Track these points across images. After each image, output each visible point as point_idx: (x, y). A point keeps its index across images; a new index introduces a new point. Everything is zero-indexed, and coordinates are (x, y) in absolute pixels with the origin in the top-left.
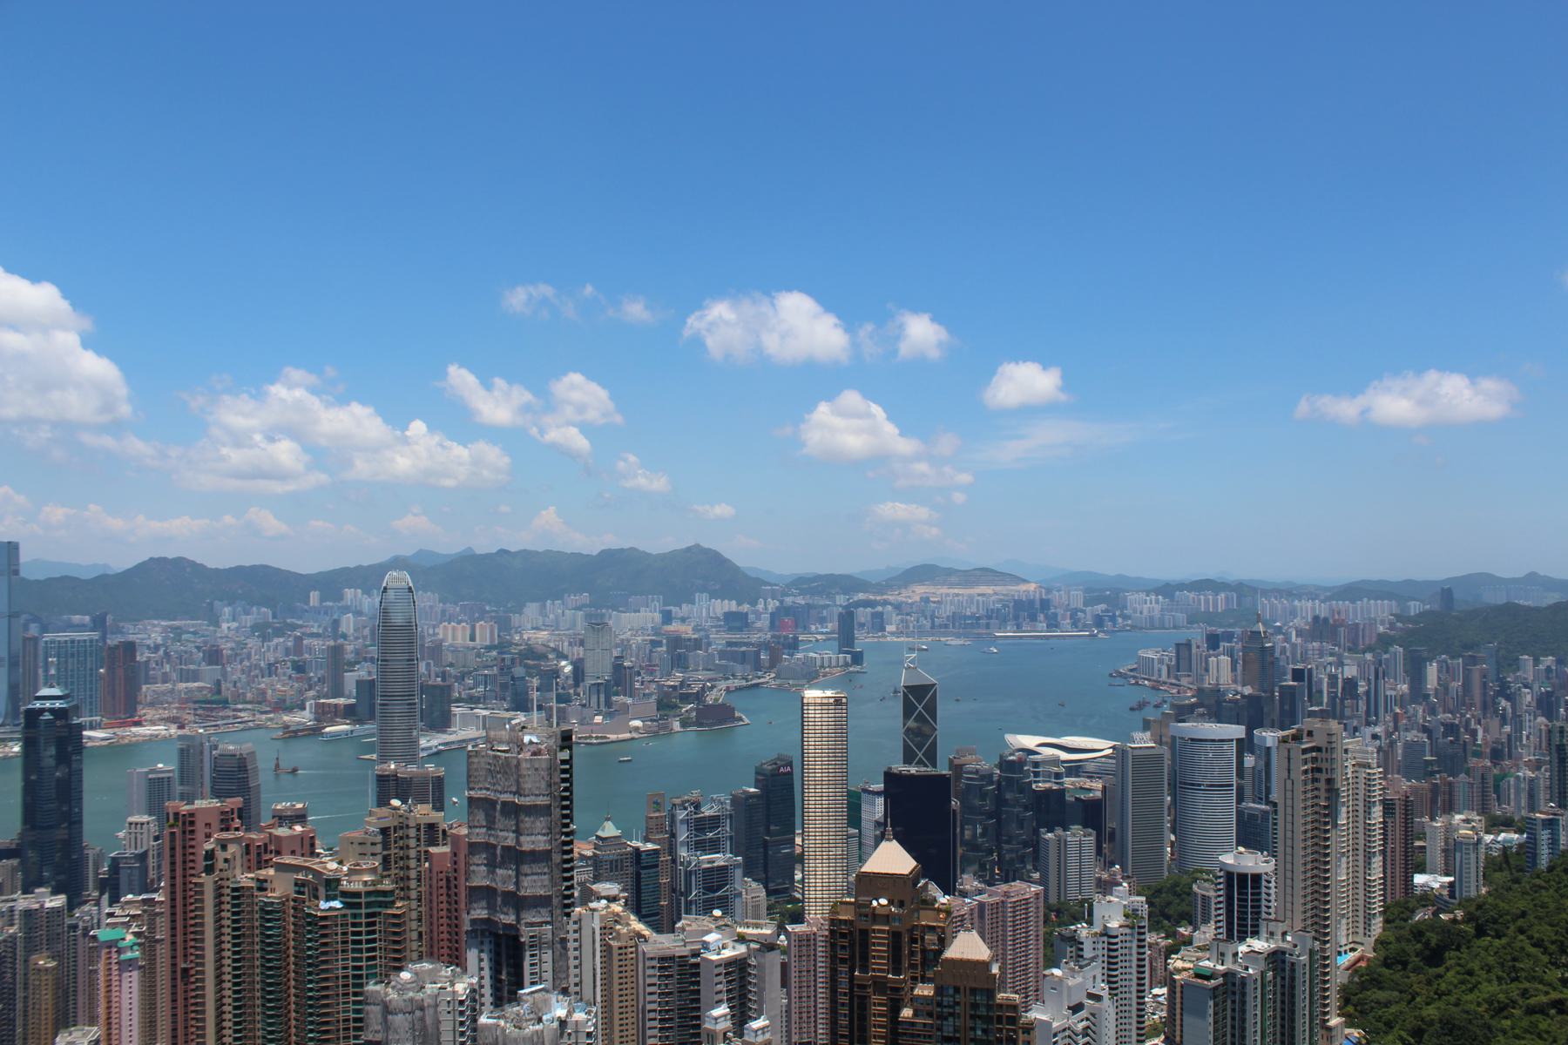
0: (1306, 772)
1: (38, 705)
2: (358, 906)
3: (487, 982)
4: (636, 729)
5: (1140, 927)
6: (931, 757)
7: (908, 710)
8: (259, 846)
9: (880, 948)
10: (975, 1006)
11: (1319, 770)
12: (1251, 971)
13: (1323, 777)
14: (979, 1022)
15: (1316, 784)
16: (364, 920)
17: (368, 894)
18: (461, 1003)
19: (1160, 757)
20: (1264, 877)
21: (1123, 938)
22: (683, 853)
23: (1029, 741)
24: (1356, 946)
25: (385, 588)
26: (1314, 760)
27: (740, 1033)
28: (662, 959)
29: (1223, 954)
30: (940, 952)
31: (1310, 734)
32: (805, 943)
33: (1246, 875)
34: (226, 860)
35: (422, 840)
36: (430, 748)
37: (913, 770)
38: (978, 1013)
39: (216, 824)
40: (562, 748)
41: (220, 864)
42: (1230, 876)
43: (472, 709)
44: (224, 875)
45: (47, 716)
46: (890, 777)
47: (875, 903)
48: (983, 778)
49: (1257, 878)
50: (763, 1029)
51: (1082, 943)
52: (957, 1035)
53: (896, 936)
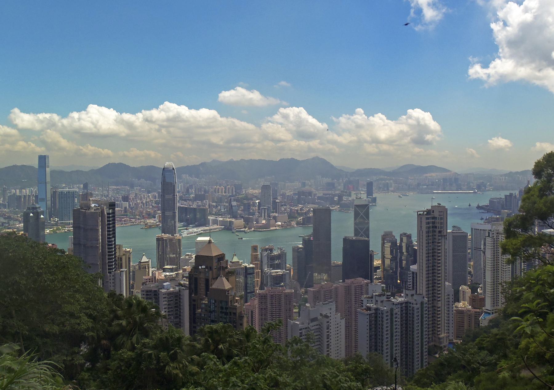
0: (429, 228)
4: (279, 226)
5: (387, 295)
9: (202, 285)
10: (222, 308)
11: (436, 227)
13: (437, 230)
14: (223, 314)
15: (435, 234)
26: (434, 223)
28: (147, 291)
29: (377, 301)
32: (263, 297)
36: (198, 232)
38: (223, 311)
43: (216, 218)
47: (200, 267)
51: (363, 301)
52: (216, 319)
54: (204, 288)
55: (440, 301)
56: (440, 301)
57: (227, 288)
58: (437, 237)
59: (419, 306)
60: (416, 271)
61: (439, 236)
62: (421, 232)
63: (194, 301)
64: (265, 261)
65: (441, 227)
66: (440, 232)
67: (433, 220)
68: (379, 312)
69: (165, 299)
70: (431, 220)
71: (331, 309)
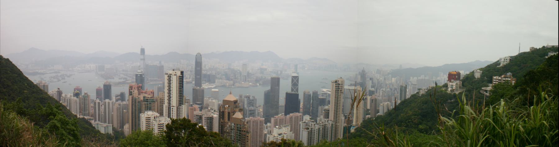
1: (137, 73)
2: (148, 101)
6: (297, 90)
7: (293, 81)
11: (339, 89)
12: (316, 128)
13: (340, 90)
26: (338, 86)
29: (312, 125)
41: (133, 94)
45: (139, 75)
46: (287, 94)
55: (339, 123)
56: (339, 123)
59: (331, 125)
61: (340, 93)
65: (342, 89)
66: (341, 91)
68: (313, 130)
70: (337, 85)
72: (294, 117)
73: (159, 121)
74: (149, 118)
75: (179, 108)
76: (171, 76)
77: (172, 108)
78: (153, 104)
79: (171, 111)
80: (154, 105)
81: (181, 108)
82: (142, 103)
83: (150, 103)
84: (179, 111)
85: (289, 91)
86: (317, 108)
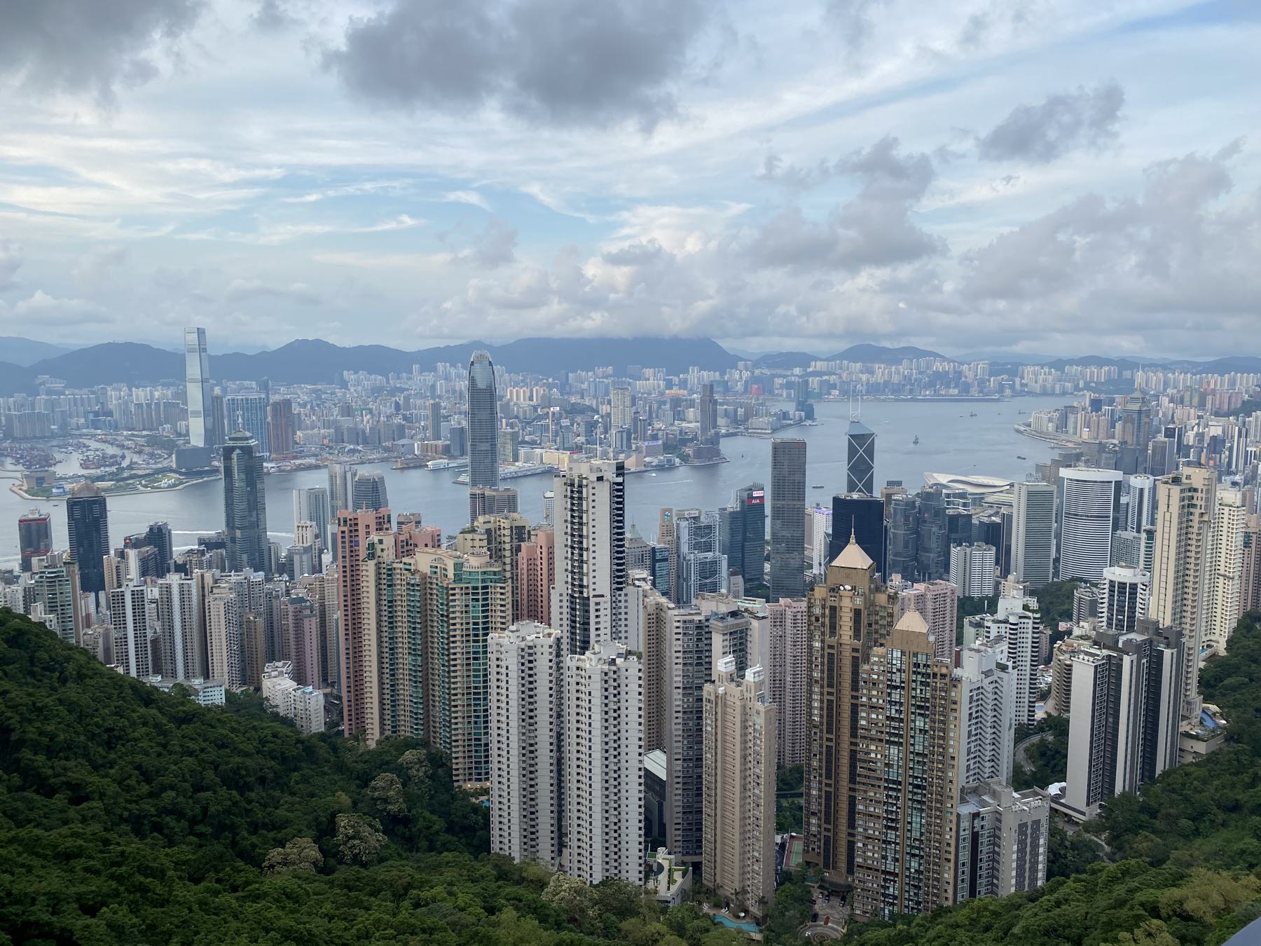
0: (1183, 506)
1: (231, 444)
3: (566, 634)
6: (869, 487)
7: (852, 451)
8: (402, 541)
10: (917, 665)
11: (1194, 506)
13: (1197, 511)
14: (919, 676)
15: (1191, 517)
16: (480, 591)
17: (485, 573)
18: (551, 647)
19: (1051, 493)
20: (1140, 586)
21: (1022, 626)
22: (685, 549)
23: (943, 479)
24: (1215, 644)
25: (472, 363)
27: (743, 677)
28: (685, 622)
30: (890, 624)
31: (1188, 477)
33: (1125, 584)
34: (382, 550)
35: (514, 536)
37: (855, 496)
39: (373, 527)
40: (618, 475)
41: (379, 553)
42: (1112, 583)
44: (381, 560)
47: (842, 588)
48: (907, 504)
49: (1134, 587)
50: (758, 672)
53: (857, 613)
54: (851, 624)
57: (925, 631)
58: (1196, 524)
60: (1133, 581)
62: (1168, 515)
63: (830, 647)
64: (685, 536)
67: (1190, 494)
69: (726, 637)
71: (1002, 652)
72: (929, 596)
73: (600, 659)
74: (530, 647)
75: (614, 599)
76: (585, 482)
77: (597, 604)
78: (498, 590)
79: (592, 614)
80: (502, 594)
81: (622, 598)
82: (454, 589)
83: (486, 587)
84: (614, 611)
85: (843, 493)
86: (947, 554)
